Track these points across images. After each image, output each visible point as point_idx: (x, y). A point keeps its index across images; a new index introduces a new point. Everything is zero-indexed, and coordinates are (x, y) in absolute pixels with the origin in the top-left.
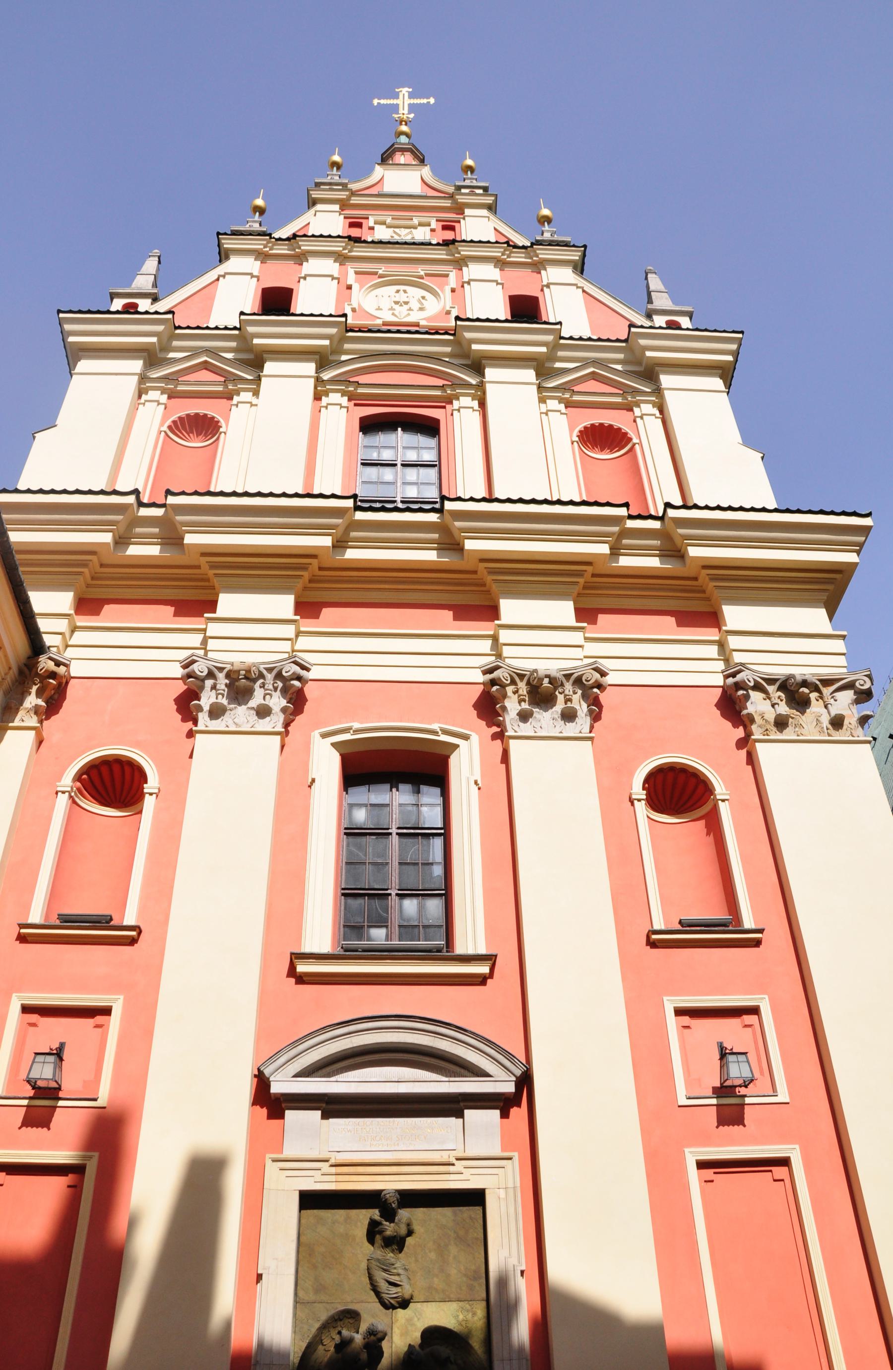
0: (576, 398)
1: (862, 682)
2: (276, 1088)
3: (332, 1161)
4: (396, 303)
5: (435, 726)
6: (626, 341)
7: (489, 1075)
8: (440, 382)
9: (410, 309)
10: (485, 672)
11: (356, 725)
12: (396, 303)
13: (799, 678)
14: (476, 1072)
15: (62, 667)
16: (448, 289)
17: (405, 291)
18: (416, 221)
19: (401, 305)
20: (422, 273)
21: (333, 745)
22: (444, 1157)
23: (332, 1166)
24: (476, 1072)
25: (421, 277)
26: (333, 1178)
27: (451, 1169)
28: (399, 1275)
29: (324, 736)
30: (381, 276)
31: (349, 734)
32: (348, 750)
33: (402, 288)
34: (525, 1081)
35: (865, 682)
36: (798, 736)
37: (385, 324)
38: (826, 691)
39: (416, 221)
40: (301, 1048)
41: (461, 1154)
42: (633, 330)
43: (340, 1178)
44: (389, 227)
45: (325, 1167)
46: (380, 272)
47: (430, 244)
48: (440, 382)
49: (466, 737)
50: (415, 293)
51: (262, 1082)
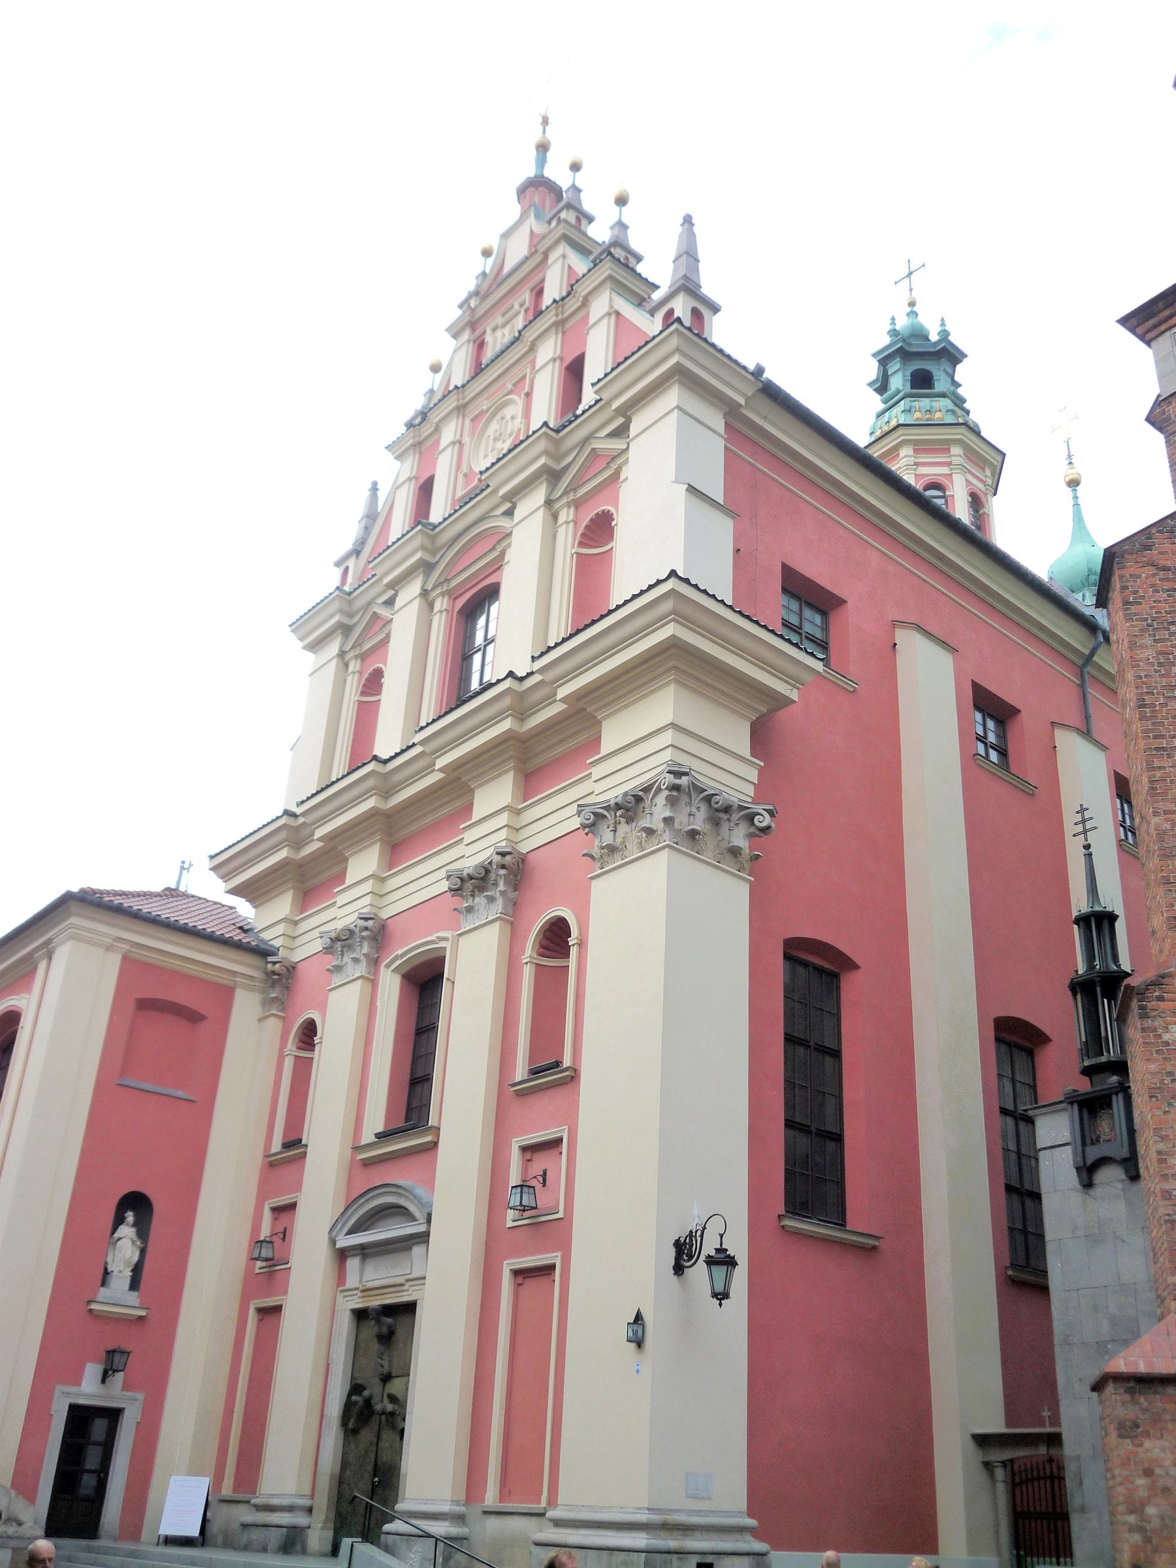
11: (400, 952)
15: (277, 966)
16: (523, 395)
29: (387, 966)
33: (498, 417)
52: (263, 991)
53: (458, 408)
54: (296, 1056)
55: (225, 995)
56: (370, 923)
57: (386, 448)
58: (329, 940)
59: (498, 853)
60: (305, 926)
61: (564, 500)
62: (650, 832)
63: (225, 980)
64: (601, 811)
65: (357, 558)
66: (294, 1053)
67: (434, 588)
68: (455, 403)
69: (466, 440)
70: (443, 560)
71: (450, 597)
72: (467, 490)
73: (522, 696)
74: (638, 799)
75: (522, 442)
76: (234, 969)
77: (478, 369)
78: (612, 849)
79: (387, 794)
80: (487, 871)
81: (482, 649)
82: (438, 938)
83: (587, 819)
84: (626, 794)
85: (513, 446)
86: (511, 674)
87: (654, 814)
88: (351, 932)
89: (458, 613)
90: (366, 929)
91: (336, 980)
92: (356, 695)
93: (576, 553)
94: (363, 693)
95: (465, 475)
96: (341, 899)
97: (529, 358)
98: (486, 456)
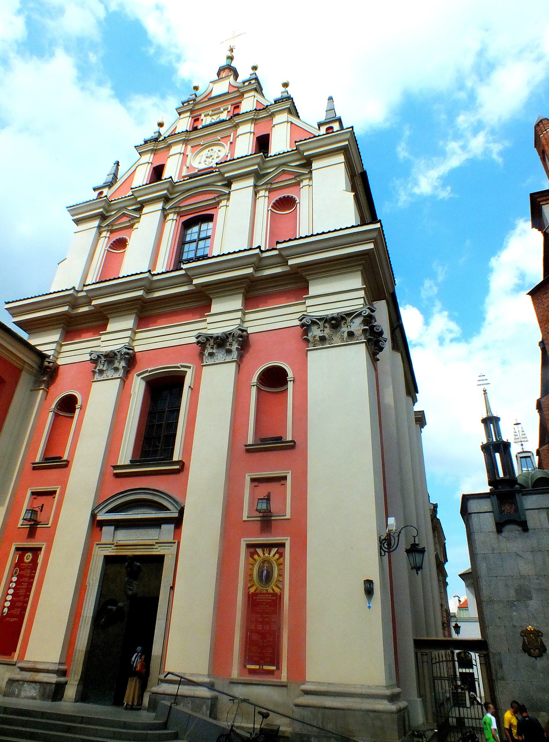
0: (274, 186)
1: (364, 312)
2: (99, 518)
3: (115, 544)
4: (207, 157)
5: (178, 365)
6: (296, 149)
7: (169, 510)
8: (212, 196)
9: (213, 159)
10: (197, 338)
11: (149, 369)
12: (207, 157)
13: (330, 316)
14: (166, 509)
15: (51, 364)
16: (229, 143)
17: (212, 150)
18: (222, 109)
19: (209, 158)
20: (219, 138)
21: (141, 378)
22: (153, 542)
23: (115, 546)
24: (166, 509)
25: (219, 140)
26: (115, 551)
27: (154, 547)
28: (132, 586)
29: (138, 375)
30: (202, 145)
31: (147, 373)
32: (149, 379)
33: (210, 149)
34: (181, 512)
35: (366, 311)
36: (330, 344)
37: (199, 171)
38: (349, 319)
39: (222, 109)
40: (108, 502)
41: (157, 541)
42: (297, 144)
43: (117, 551)
44: (211, 116)
45: (113, 547)
46: (201, 143)
47: (226, 121)
48: (212, 196)
49: (189, 367)
50: (216, 148)
51: (93, 516)
52: (35, 376)
53: (184, 140)
54: (56, 413)
55: (17, 373)
56: (131, 351)
57: (135, 147)
58: (96, 357)
59: (239, 329)
60: (64, 348)
61: (264, 187)
62: (351, 334)
63: (17, 364)
64: (344, 316)
65: (109, 189)
66: (56, 411)
67: (169, 209)
68: (184, 138)
69: (188, 152)
70: (178, 197)
71: (178, 215)
72: (187, 174)
73: (261, 259)
74: (343, 318)
75: (226, 162)
76: (26, 360)
77: (195, 129)
78: (323, 339)
79: (257, 268)
80: (227, 338)
81: (197, 241)
82: (181, 365)
83: (308, 322)
84: (338, 314)
85: (220, 162)
86: (259, 247)
87: (352, 326)
88: (115, 354)
89: (183, 223)
90: (128, 354)
91: (97, 377)
92: (106, 247)
93: (271, 210)
94: (110, 247)
95: (188, 167)
96: (103, 338)
97: (234, 129)
98: (200, 163)
